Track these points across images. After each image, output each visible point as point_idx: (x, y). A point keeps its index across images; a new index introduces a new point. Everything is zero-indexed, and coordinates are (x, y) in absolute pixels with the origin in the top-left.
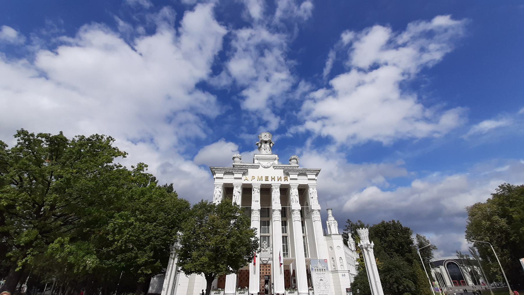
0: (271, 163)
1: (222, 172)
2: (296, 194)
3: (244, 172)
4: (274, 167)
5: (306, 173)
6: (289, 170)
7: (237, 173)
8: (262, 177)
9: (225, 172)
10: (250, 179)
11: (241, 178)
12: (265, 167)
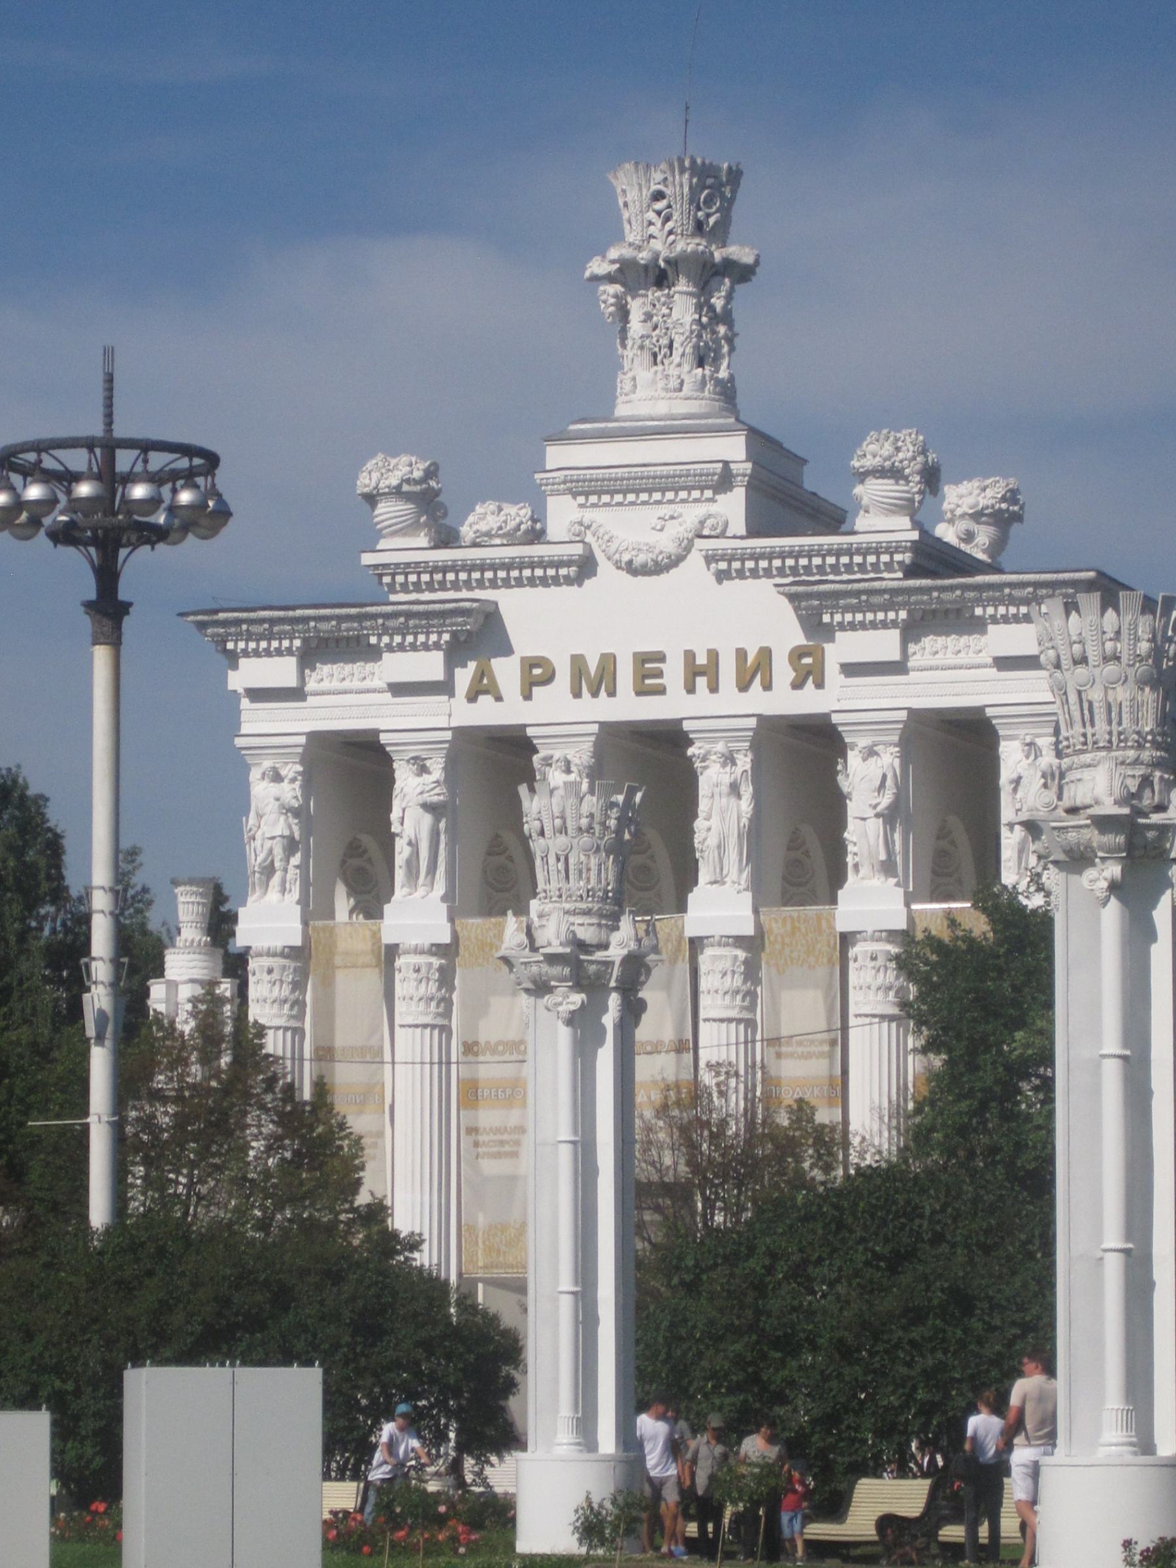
0: (691, 514)
2: (875, 807)
4: (710, 559)
7: (401, 648)
8: (608, 662)
12: (633, 569)
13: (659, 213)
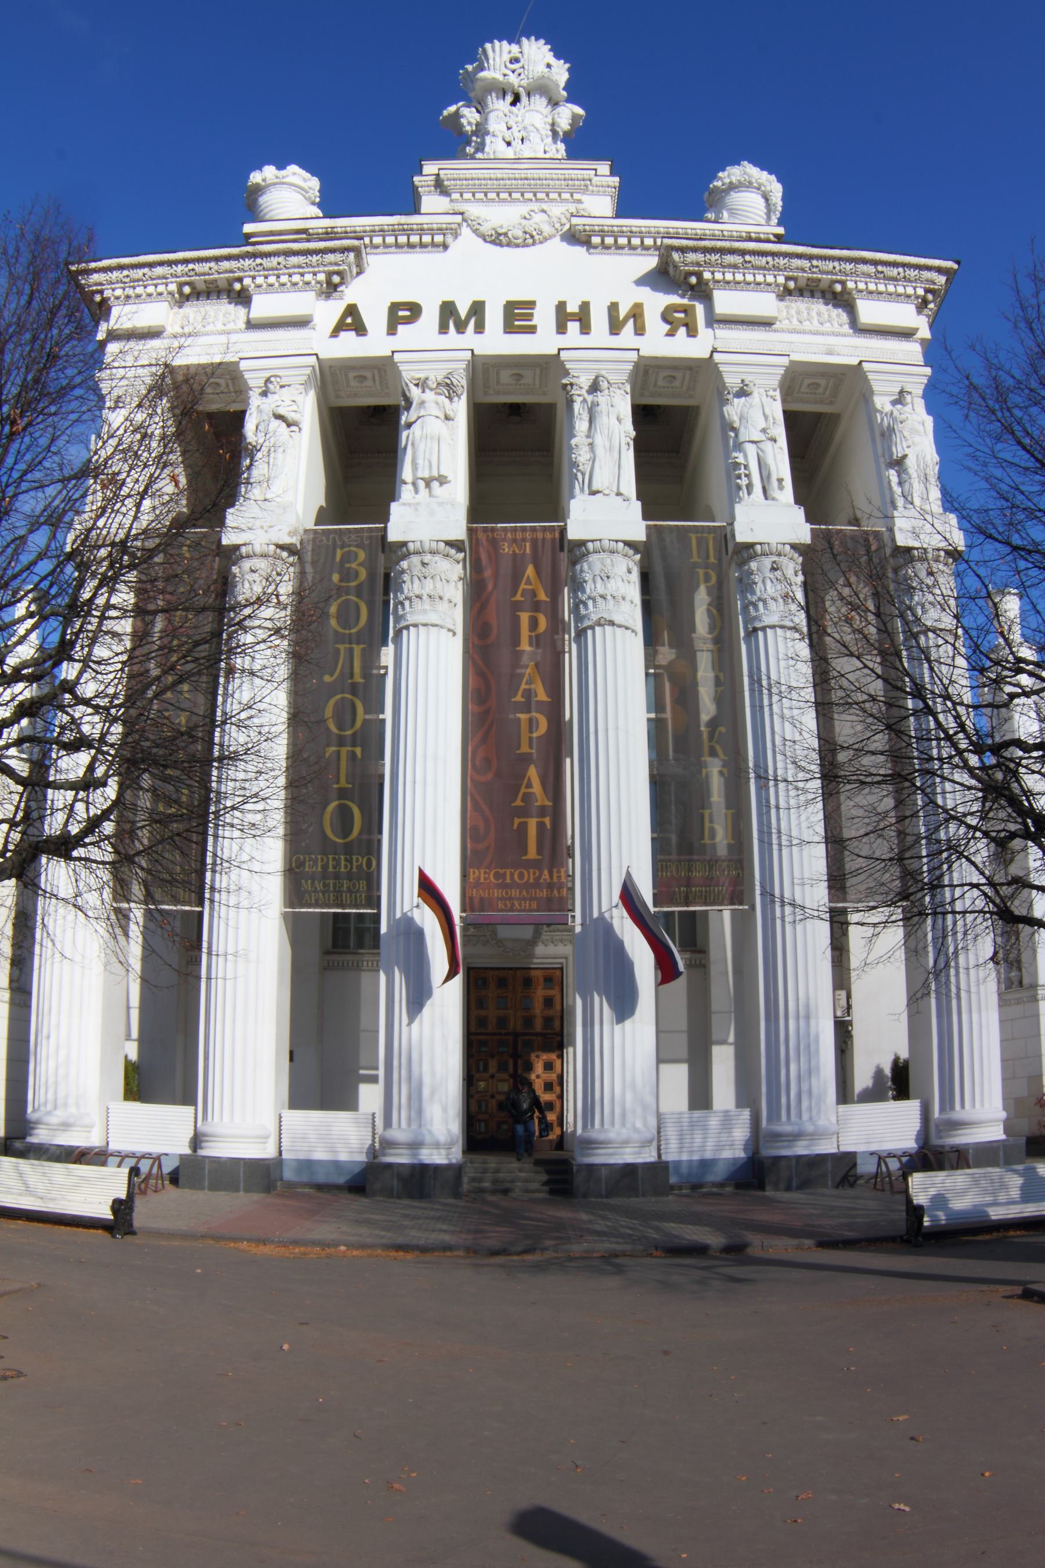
1: (161, 288)
2: (764, 431)
3: (329, 275)
5: (843, 283)
6: (706, 251)
8: (478, 309)
9: (181, 285)
10: (375, 318)
11: (302, 323)
13: (513, 72)
